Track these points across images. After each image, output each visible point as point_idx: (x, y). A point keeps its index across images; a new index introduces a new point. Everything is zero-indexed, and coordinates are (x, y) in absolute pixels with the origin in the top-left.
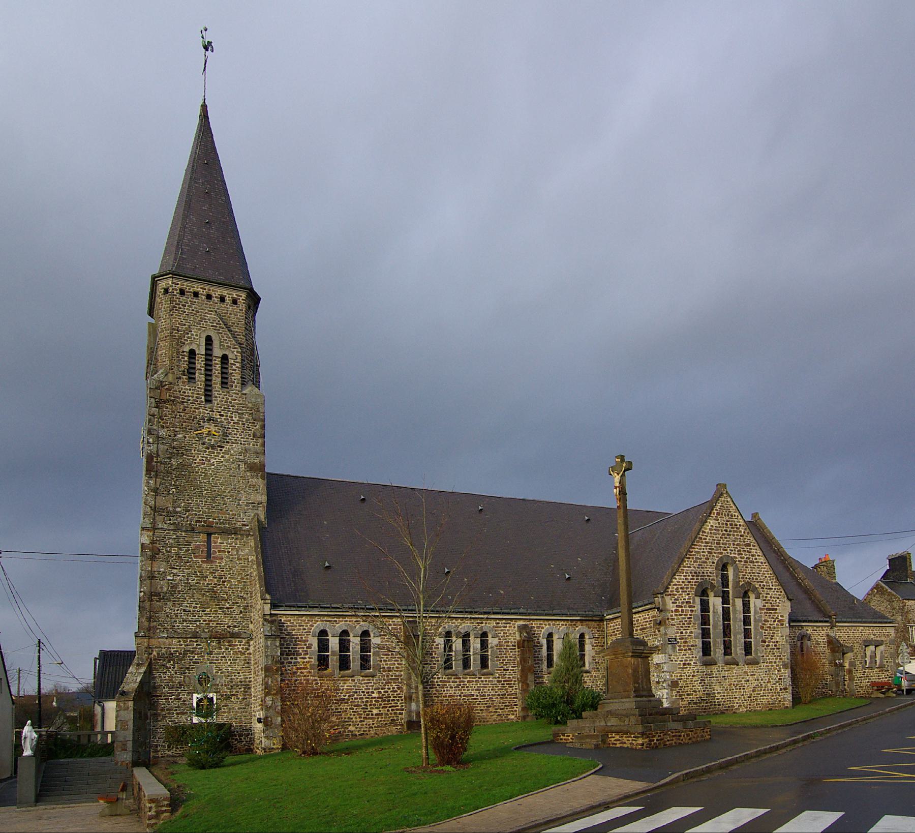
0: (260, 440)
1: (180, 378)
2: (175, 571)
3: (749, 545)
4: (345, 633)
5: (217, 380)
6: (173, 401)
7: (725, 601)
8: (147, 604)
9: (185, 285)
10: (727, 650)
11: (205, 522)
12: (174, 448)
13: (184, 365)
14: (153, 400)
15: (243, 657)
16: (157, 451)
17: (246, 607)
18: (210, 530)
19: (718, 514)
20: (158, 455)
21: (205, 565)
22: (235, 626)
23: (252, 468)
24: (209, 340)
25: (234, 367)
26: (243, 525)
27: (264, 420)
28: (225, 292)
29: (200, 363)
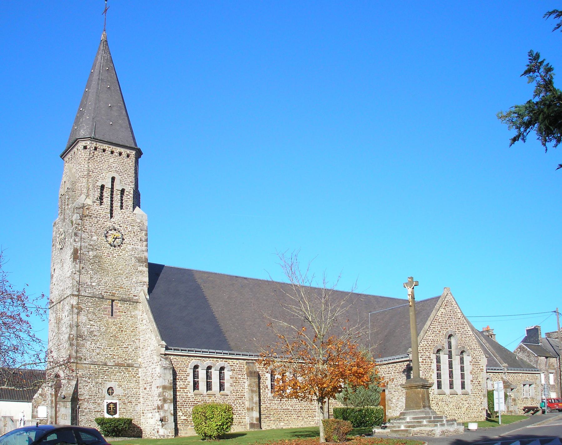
0: (145, 243)
1: (95, 202)
2: (92, 322)
3: (463, 324)
4: (209, 368)
5: (117, 204)
6: (91, 216)
7: (450, 357)
8: (75, 342)
9: (99, 145)
10: (451, 386)
11: (110, 293)
12: (91, 245)
13: (97, 194)
14: (78, 215)
15: (135, 379)
16: (81, 246)
17: (136, 348)
18: (113, 299)
19: (446, 305)
20: (81, 249)
21: (110, 320)
22: (129, 359)
23: (140, 260)
24: (113, 179)
25: (129, 197)
26: (134, 296)
27: (147, 231)
28: (122, 150)
29: (107, 193)
